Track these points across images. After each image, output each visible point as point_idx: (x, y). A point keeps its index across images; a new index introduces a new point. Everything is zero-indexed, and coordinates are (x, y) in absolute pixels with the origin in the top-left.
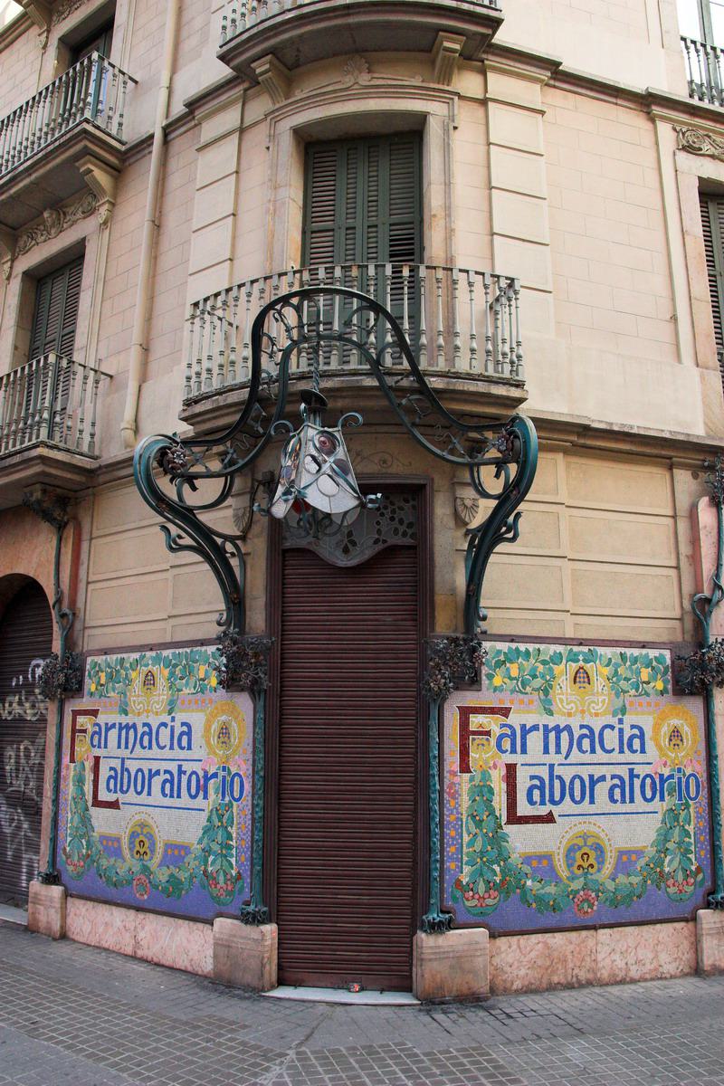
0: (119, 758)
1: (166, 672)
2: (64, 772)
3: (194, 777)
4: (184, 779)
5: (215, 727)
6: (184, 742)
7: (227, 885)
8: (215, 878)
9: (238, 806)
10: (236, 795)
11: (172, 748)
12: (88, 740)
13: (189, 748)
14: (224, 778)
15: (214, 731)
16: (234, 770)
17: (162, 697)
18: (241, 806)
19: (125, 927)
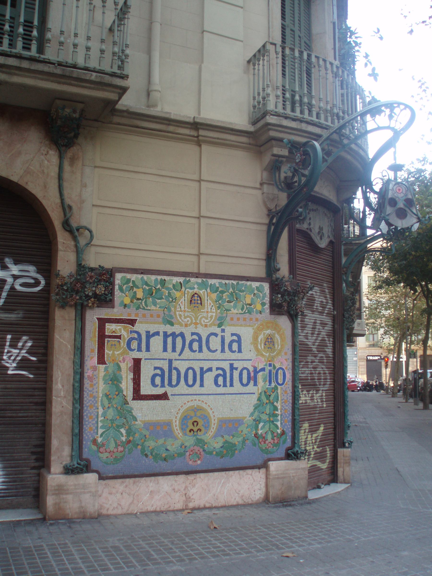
0: (166, 359)
1: (214, 296)
2: (88, 373)
3: (245, 373)
4: (236, 374)
5: (261, 337)
6: (235, 346)
7: (274, 440)
8: (264, 438)
9: (282, 388)
10: (280, 381)
11: (223, 351)
12: (123, 343)
13: (240, 351)
14: (270, 371)
15: (261, 340)
16: (278, 366)
17: (210, 314)
18: (284, 389)
19: (174, 489)
